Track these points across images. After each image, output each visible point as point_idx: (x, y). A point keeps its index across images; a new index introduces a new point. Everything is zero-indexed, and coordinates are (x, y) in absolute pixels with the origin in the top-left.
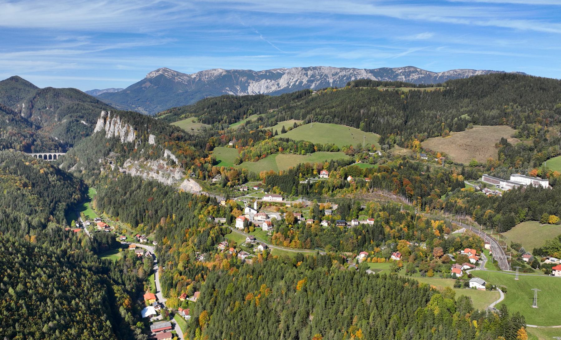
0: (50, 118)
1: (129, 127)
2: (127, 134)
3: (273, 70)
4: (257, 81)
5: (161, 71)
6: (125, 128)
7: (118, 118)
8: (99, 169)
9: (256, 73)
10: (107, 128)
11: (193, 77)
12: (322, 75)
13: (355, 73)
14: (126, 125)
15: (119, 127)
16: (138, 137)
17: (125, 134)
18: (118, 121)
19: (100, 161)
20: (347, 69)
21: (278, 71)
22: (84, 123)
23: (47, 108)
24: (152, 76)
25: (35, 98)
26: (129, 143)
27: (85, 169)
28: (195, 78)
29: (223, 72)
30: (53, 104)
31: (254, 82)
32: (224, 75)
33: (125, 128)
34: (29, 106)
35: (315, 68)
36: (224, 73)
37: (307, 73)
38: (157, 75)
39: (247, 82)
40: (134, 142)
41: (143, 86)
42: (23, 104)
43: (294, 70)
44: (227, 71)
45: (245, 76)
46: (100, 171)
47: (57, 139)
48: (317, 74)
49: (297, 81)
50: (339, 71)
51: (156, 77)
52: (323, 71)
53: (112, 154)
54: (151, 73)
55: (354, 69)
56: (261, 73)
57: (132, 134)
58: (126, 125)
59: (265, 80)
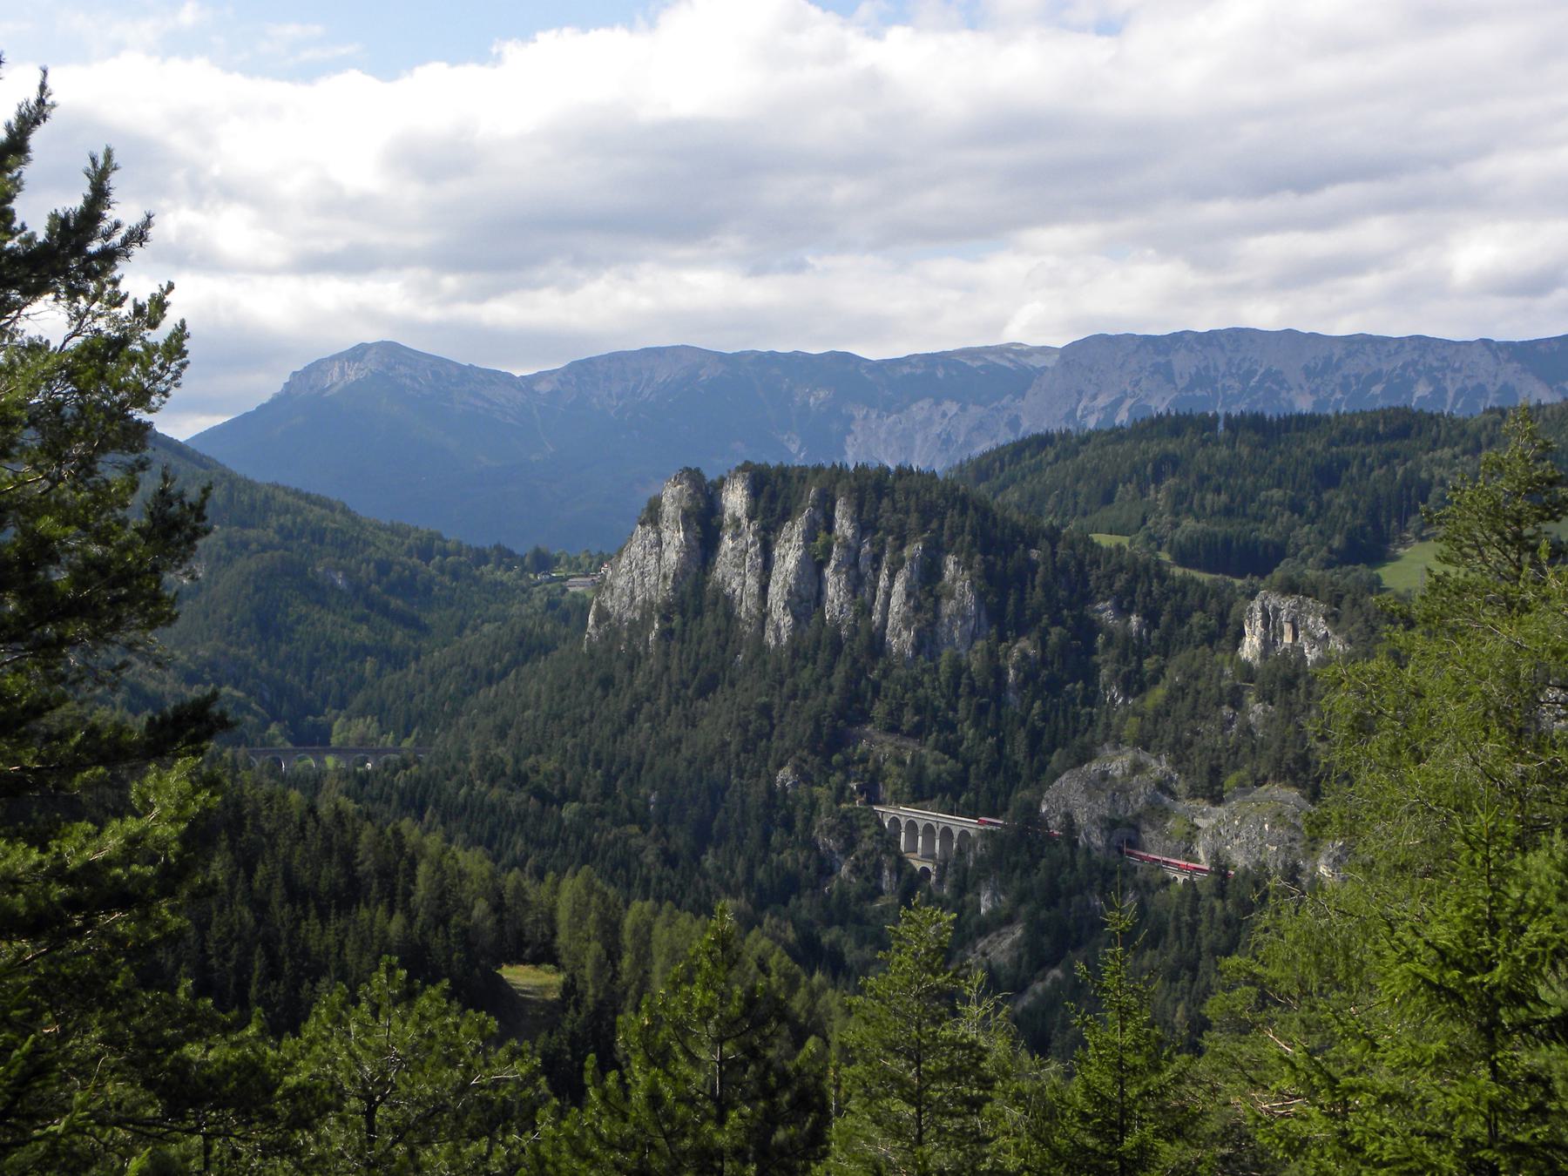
12: (1250, 373)
18: (844, 526)
21: (990, 358)
38: (352, 376)
48: (1222, 368)
49: (1117, 404)
59: (932, 400)
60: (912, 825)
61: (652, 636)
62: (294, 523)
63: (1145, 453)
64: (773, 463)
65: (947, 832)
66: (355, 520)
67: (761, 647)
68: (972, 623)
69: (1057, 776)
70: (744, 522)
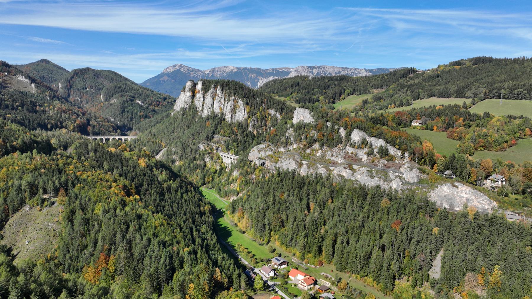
0: (92, 99)
1: (237, 102)
2: (234, 110)
3: (279, 68)
4: (265, 78)
5: (177, 66)
6: (231, 103)
7: (219, 88)
8: (203, 159)
9: (264, 71)
10: (198, 103)
11: (207, 73)
13: (356, 72)
14: (232, 98)
15: (220, 101)
16: (251, 114)
17: (232, 111)
18: (219, 92)
19: (202, 148)
20: (349, 68)
22: (140, 103)
23: (87, 89)
24: (169, 71)
25: (72, 77)
26: (240, 124)
27: (181, 158)
28: (208, 73)
29: (234, 69)
30: (94, 85)
32: (235, 72)
33: (231, 103)
34: (67, 86)
35: (319, 67)
36: (235, 70)
37: (313, 72)
38: (174, 70)
39: (256, 78)
40: (246, 120)
41: (161, 79)
42: (60, 84)
43: (300, 68)
44: (237, 68)
45: (254, 73)
46: (205, 162)
47: (112, 120)
50: (341, 70)
51: (173, 72)
52: (327, 70)
53: (217, 137)
54: (168, 68)
55: (355, 69)
56: (269, 71)
57: (243, 111)
58: (232, 98)
62: (137, 92)
63: (294, 82)
65: (231, 158)
67: (201, 117)
68: (243, 113)
70: (201, 91)
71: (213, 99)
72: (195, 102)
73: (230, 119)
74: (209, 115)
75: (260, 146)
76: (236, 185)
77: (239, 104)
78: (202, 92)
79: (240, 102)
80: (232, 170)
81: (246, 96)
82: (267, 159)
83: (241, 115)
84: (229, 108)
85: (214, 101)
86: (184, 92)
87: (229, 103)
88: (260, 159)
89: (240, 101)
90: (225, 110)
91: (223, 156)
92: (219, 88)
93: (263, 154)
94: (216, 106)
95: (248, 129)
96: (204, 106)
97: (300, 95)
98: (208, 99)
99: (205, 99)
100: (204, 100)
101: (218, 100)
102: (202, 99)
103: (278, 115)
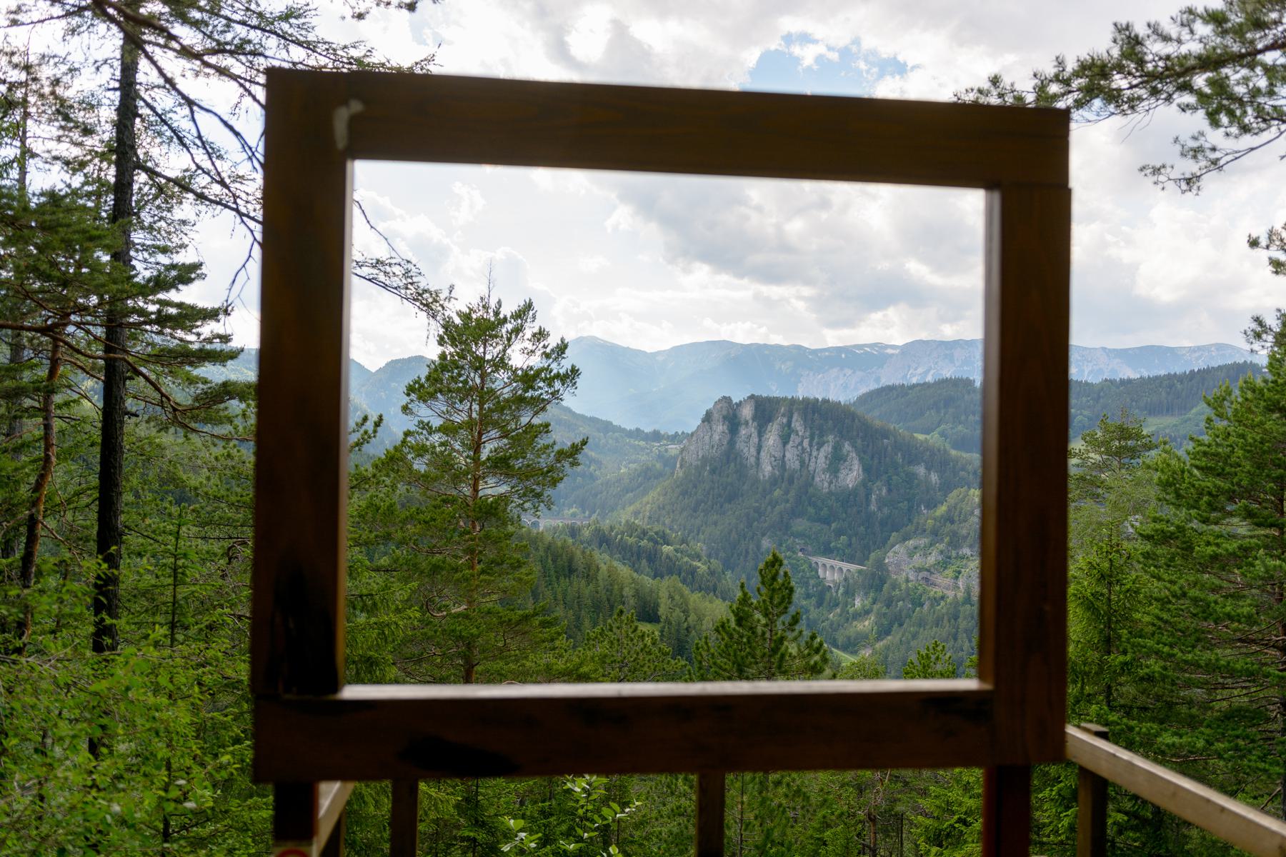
15: (801, 443)
18: (797, 424)
31: (811, 374)
33: (827, 449)
49: (926, 373)
60: (824, 565)
61: (706, 473)
64: (764, 395)
65: (841, 569)
66: (574, 413)
68: (855, 473)
69: (893, 546)
70: (750, 422)
71: (785, 440)
72: (737, 446)
73: (826, 484)
74: (773, 475)
75: (911, 543)
76: (867, 623)
77: (844, 451)
78: (755, 424)
79: (847, 447)
80: (849, 593)
81: (861, 434)
82: (932, 570)
83: (852, 476)
84: (821, 459)
85: (785, 443)
86: (709, 422)
87: (822, 450)
88: (920, 570)
89: (846, 446)
90: (812, 464)
91: (820, 564)
92: (795, 417)
93: (918, 560)
94: (791, 454)
95: (868, 505)
96: (762, 454)
97: (960, 427)
98: (772, 439)
99: (763, 439)
100: (760, 440)
101: (797, 442)
102: (756, 440)
103: (934, 477)
